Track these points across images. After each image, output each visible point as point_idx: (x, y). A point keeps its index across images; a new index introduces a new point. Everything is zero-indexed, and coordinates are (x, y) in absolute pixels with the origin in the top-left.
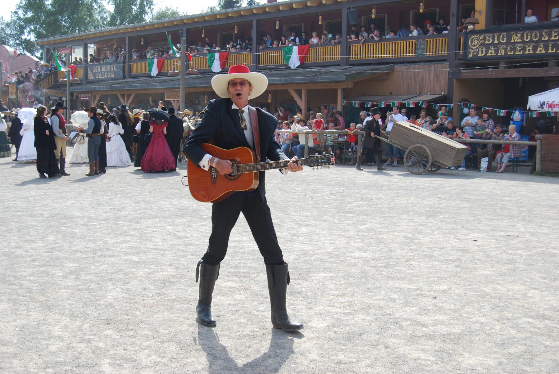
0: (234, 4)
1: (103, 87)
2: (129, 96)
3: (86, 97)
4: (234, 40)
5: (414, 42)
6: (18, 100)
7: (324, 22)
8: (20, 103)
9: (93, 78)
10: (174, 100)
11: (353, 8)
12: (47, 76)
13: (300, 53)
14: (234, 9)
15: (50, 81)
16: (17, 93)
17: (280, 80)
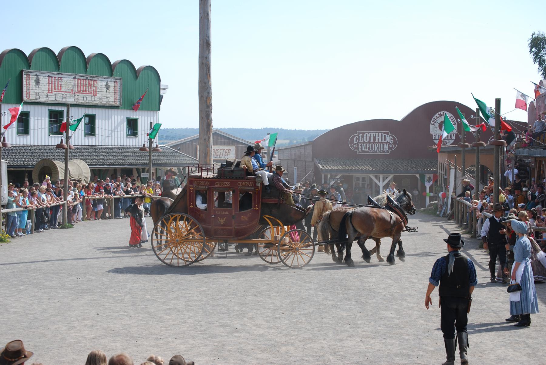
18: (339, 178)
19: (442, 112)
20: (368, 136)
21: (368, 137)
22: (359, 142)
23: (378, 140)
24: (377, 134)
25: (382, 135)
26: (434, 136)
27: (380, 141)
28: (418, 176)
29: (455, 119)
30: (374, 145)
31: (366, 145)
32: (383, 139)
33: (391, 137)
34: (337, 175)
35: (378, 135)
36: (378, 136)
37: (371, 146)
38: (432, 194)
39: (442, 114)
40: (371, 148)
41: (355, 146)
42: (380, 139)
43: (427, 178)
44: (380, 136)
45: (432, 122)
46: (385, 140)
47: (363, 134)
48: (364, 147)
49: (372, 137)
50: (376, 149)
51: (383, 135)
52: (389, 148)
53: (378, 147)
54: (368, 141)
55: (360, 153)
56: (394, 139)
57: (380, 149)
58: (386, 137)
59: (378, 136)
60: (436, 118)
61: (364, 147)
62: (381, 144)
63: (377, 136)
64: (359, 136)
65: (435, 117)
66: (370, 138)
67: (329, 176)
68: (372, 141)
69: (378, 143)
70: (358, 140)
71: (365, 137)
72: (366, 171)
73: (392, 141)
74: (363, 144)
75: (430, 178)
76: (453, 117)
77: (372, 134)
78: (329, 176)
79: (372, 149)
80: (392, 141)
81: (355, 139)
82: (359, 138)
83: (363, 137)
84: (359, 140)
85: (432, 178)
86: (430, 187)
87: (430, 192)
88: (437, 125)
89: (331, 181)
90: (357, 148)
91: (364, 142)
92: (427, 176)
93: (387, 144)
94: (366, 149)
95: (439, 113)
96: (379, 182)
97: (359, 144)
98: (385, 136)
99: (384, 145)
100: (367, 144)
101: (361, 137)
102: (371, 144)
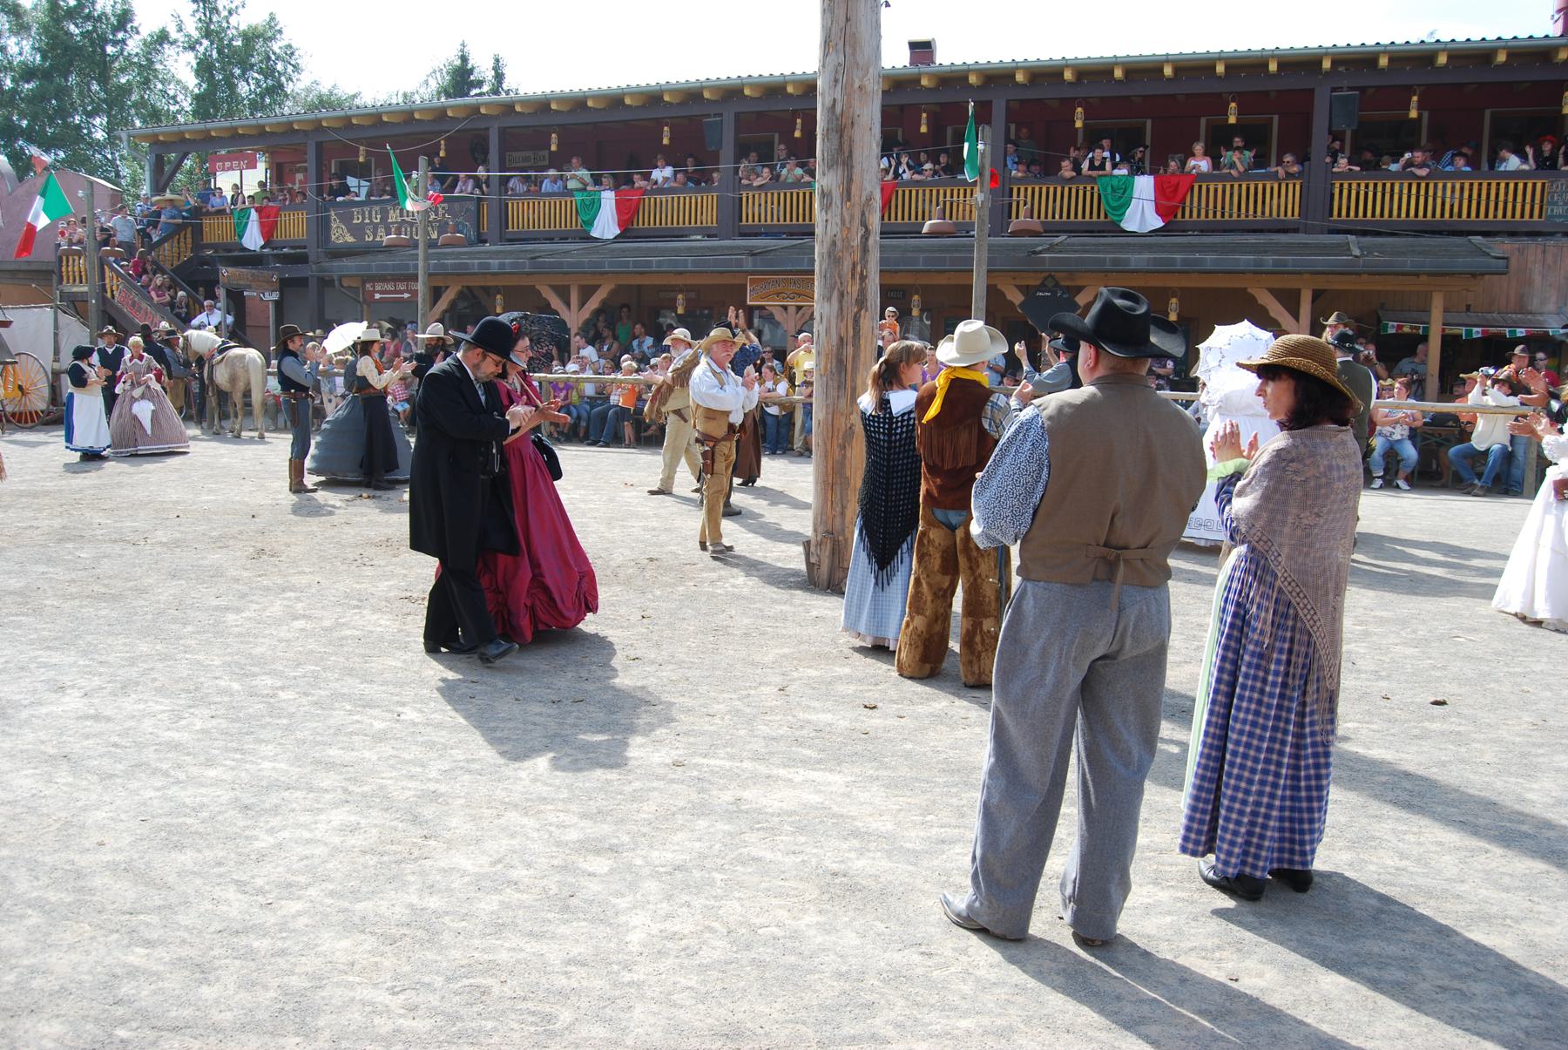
0: (469, 90)
1: (502, 265)
2: (587, 293)
3: (402, 292)
4: (1148, 142)
5: (1539, 186)
6: (104, 298)
7: (1426, 115)
8: (112, 305)
9: (350, 239)
10: (785, 308)
11: (1351, 89)
12: (174, 232)
13: (619, 205)
14: (467, 100)
15: (182, 244)
16: (103, 278)
17: (1258, 262)
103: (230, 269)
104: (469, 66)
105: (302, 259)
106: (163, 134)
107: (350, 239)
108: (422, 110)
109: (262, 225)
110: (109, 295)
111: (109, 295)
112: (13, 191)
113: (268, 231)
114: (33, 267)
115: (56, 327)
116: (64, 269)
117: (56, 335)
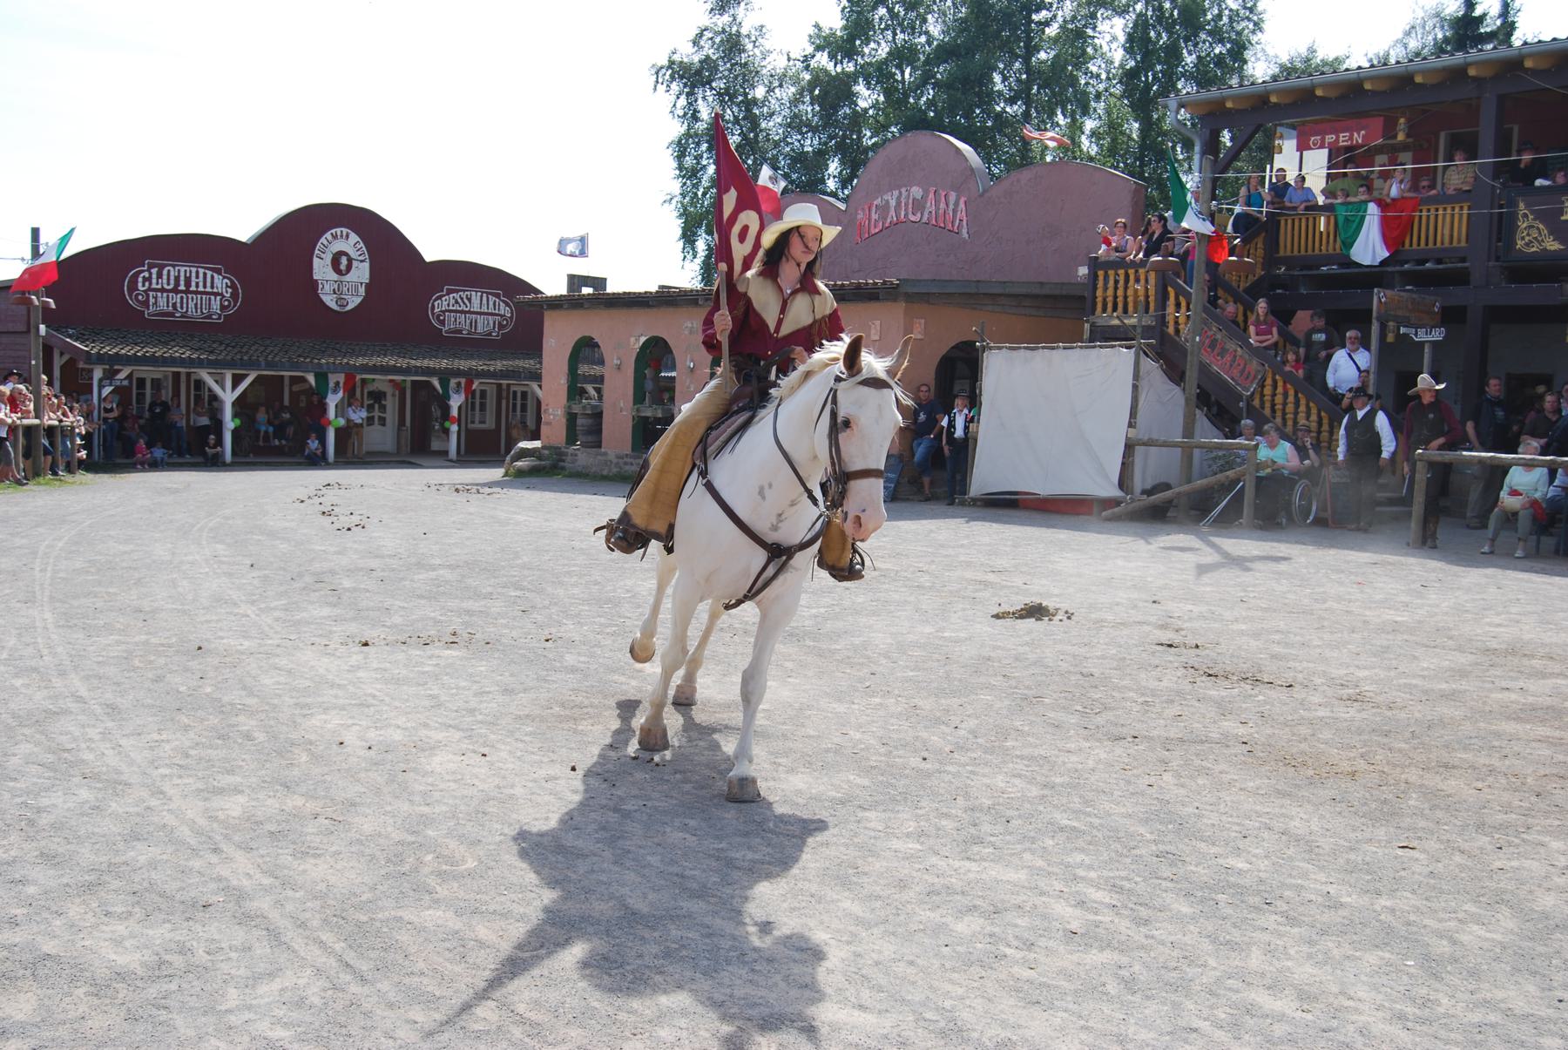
16: (1162, 304)
18: (125, 379)
19: (338, 230)
20: (172, 273)
21: (172, 278)
22: (150, 289)
23: (197, 286)
24: (194, 270)
25: (205, 274)
26: (320, 286)
27: (201, 289)
28: (311, 379)
29: (364, 249)
30: (188, 298)
31: (168, 296)
32: (209, 284)
33: (226, 280)
34: (118, 371)
35: (197, 272)
36: (197, 277)
37: (179, 300)
38: (342, 422)
39: (339, 233)
40: (178, 305)
41: (140, 297)
42: (201, 284)
43: (331, 385)
44: (201, 275)
45: (317, 252)
46: (212, 287)
47: (161, 268)
48: (162, 302)
49: (182, 278)
50: (191, 307)
51: (209, 273)
52: (223, 308)
53: (196, 304)
54: (171, 287)
55: (153, 315)
56: (233, 286)
57: (201, 308)
58: (216, 281)
59: (197, 277)
60: (325, 243)
61: (162, 302)
62: (204, 297)
63: (194, 275)
64: (151, 274)
65: (323, 240)
66: (177, 279)
67: (98, 374)
68: (182, 287)
69: (197, 293)
70: (147, 284)
71: (165, 277)
72: (182, 362)
73: (229, 290)
74: (159, 294)
75: (337, 383)
76: (362, 245)
77: (183, 269)
78: (98, 374)
79: (182, 308)
80: (229, 290)
81: (140, 280)
82: (149, 279)
83: (160, 276)
84: (151, 284)
85: (341, 385)
86: (336, 406)
87: (336, 417)
88: (328, 258)
89: (104, 386)
90: (146, 303)
91: (163, 290)
92: (332, 379)
93: (218, 298)
94: (168, 306)
95: (333, 231)
96: (224, 389)
97: (151, 293)
98: (212, 277)
99: (210, 299)
100: (171, 295)
101: (154, 276)
102: (179, 296)
103: (1389, 292)
104: (1478, 12)
105: (1460, 278)
106: (1234, 98)
107: (1553, 245)
108: (1372, 78)
109: (1386, 224)
110: (1171, 330)
111: (1171, 330)
112: (985, 191)
113: (1394, 232)
114: (1046, 291)
115: (1136, 376)
116: (1099, 293)
117: (1135, 388)
